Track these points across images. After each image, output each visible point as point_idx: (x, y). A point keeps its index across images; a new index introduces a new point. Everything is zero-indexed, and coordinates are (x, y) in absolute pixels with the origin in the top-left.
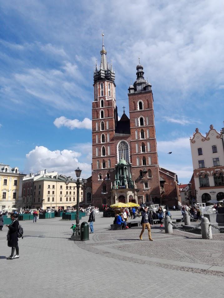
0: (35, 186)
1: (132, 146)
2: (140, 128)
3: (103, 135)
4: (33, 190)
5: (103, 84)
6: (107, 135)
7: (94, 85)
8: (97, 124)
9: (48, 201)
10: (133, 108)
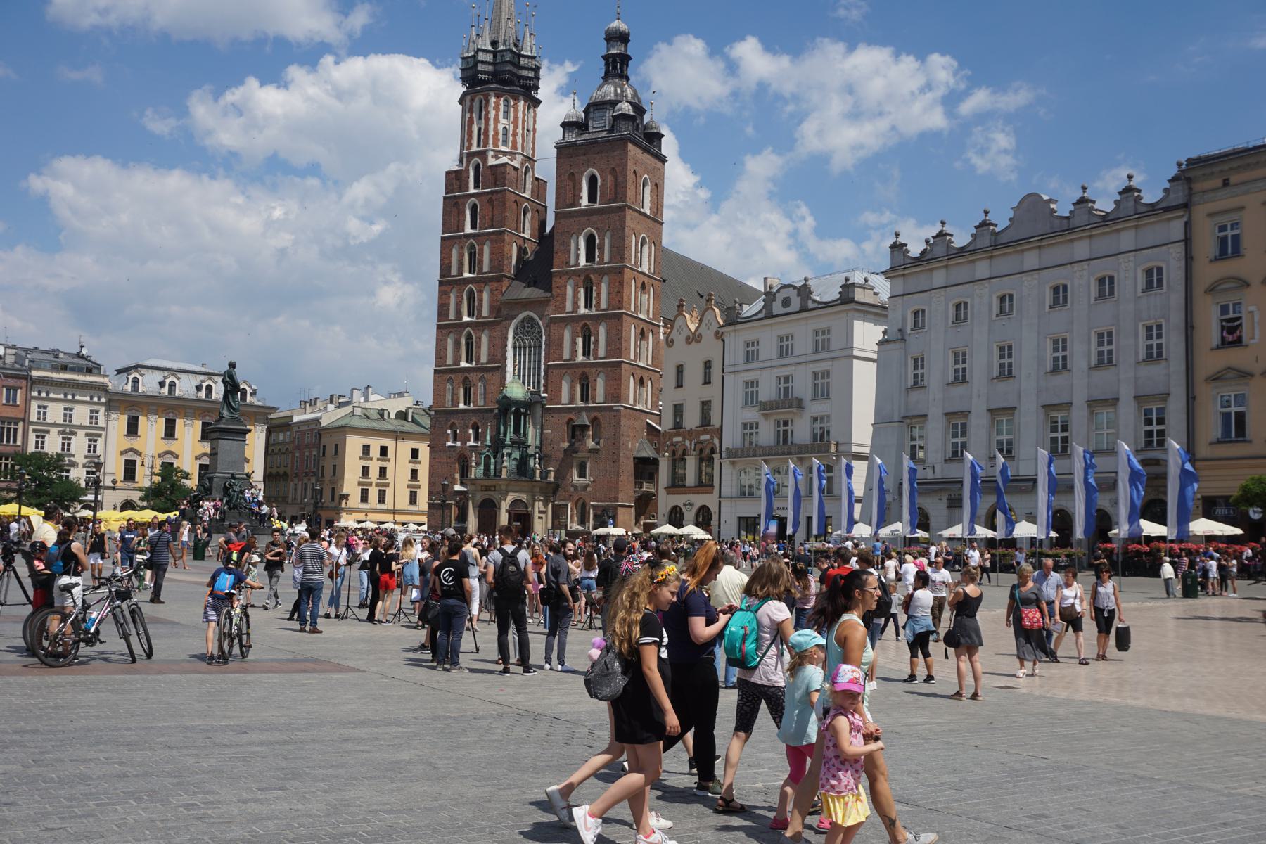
0: (324, 446)
1: (551, 334)
3: (471, 293)
4: (319, 461)
5: (484, 102)
6: (481, 292)
7: (461, 101)
8: (455, 253)
9: (362, 501)
10: (570, 195)
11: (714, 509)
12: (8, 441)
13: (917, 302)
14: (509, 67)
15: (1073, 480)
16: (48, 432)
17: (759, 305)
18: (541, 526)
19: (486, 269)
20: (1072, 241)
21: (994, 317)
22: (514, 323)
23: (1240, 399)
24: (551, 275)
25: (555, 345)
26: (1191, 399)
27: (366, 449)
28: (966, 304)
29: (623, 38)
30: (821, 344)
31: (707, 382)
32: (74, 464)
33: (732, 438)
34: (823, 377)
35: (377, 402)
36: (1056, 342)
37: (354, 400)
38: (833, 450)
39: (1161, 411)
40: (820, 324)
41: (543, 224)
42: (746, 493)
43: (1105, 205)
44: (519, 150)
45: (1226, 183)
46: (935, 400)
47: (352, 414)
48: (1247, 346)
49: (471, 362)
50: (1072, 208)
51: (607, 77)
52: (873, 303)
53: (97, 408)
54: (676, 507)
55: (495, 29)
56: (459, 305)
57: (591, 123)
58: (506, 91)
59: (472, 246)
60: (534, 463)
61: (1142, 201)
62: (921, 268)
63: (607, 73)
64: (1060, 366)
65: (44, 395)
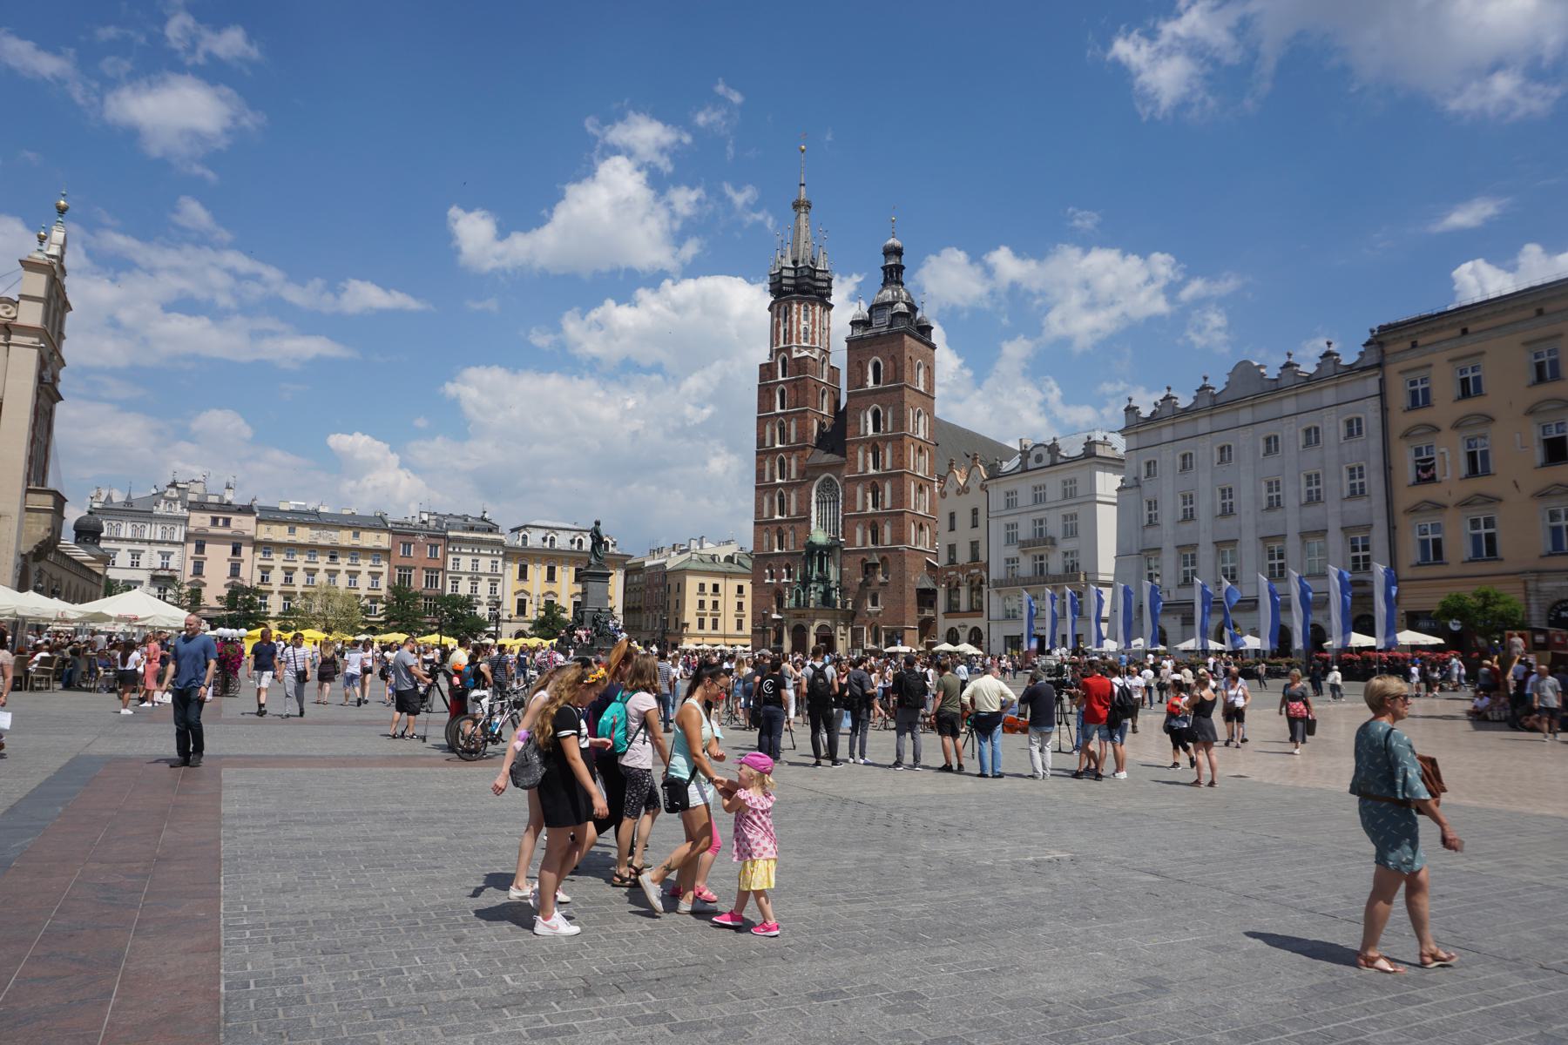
2: (871, 439)
3: (782, 460)
6: (789, 459)
7: (770, 309)
8: (768, 429)
10: (858, 378)
11: (984, 629)
12: (432, 586)
13: (1149, 454)
14: (808, 280)
15: (1289, 600)
16: (460, 578)
17: (1016, 461)
18: (842, 646)
19: (793, 441)
20: (1281, 399)
21: (1215, 465)
22: (816, 483)
23: (1436, 528)
24: (845, 444)
25: (850, 499)
26: (1392, 528)
27: (702, 586)
28: (1191, 454)
29: (898, 252)
30: (1069, 492)
31: (975, 525)
32: (480, 603)
33: (997, 571)
34: (1071, 519)
35: (709, 548)
36: (1270, 484)
37: (692, 547)
38: (1082, 579)
39: (1365, 539)
40: (1067, 476)
41: (838, 403)
42: (1011, 616)
43: (1308, 368)
44: (817, 345)
45: (1414, 345)
46: (1168, 534)
47: (691, 558)
48: (1440, 482)
50: (1280, 372)
51: (885, 285)
52: (1111, 456)
53: (496, 559)
54: (952, 628)
55: (795, 251)
56: (772, 469)
57: (874, 321)
58: (806, 299)
59: (782, 423)
60: (835, 595)
61: (1341, 363)
62: (1152, 426)
63: (886, 279)
64: (1274, 504)
65: (457, 550)
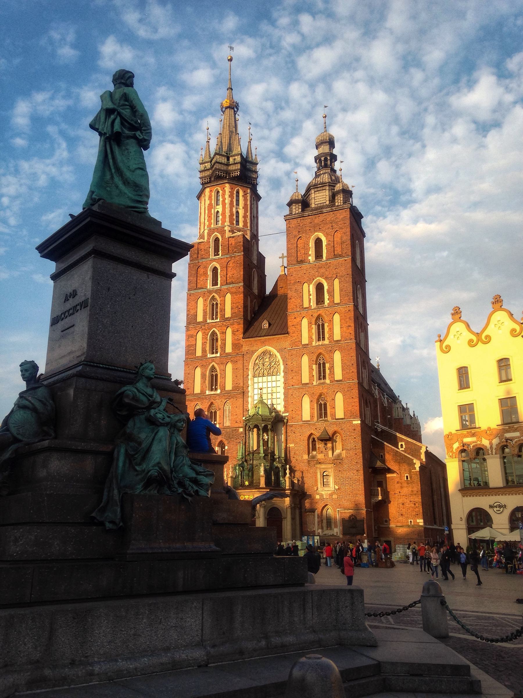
5: (221, 192)
19: (228, 314)
49: (216, 389)
56: (204, 344)
59: (213, 298)
